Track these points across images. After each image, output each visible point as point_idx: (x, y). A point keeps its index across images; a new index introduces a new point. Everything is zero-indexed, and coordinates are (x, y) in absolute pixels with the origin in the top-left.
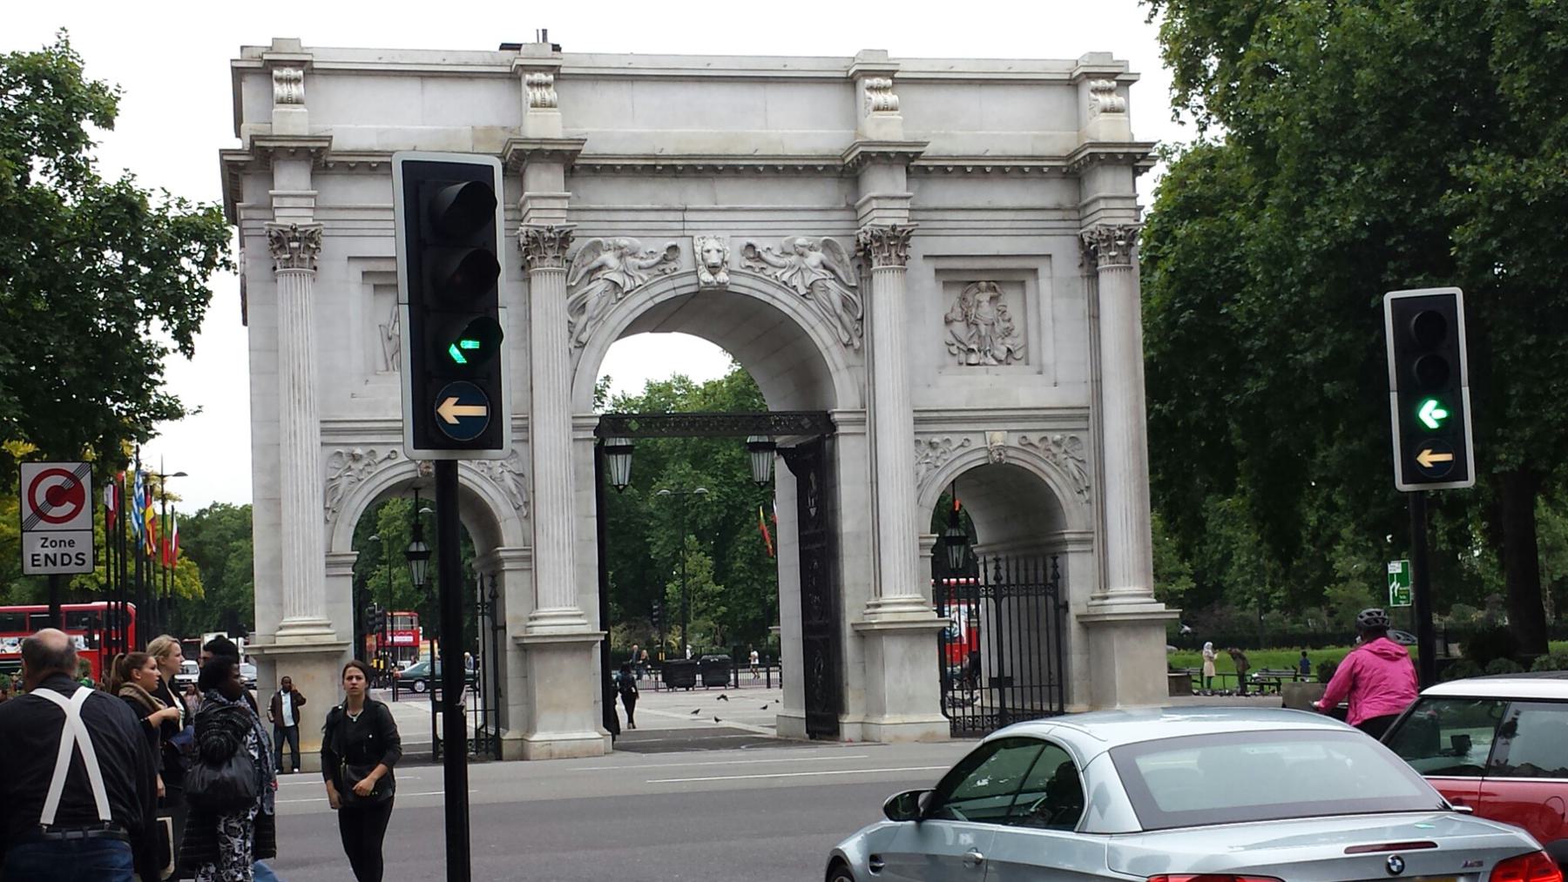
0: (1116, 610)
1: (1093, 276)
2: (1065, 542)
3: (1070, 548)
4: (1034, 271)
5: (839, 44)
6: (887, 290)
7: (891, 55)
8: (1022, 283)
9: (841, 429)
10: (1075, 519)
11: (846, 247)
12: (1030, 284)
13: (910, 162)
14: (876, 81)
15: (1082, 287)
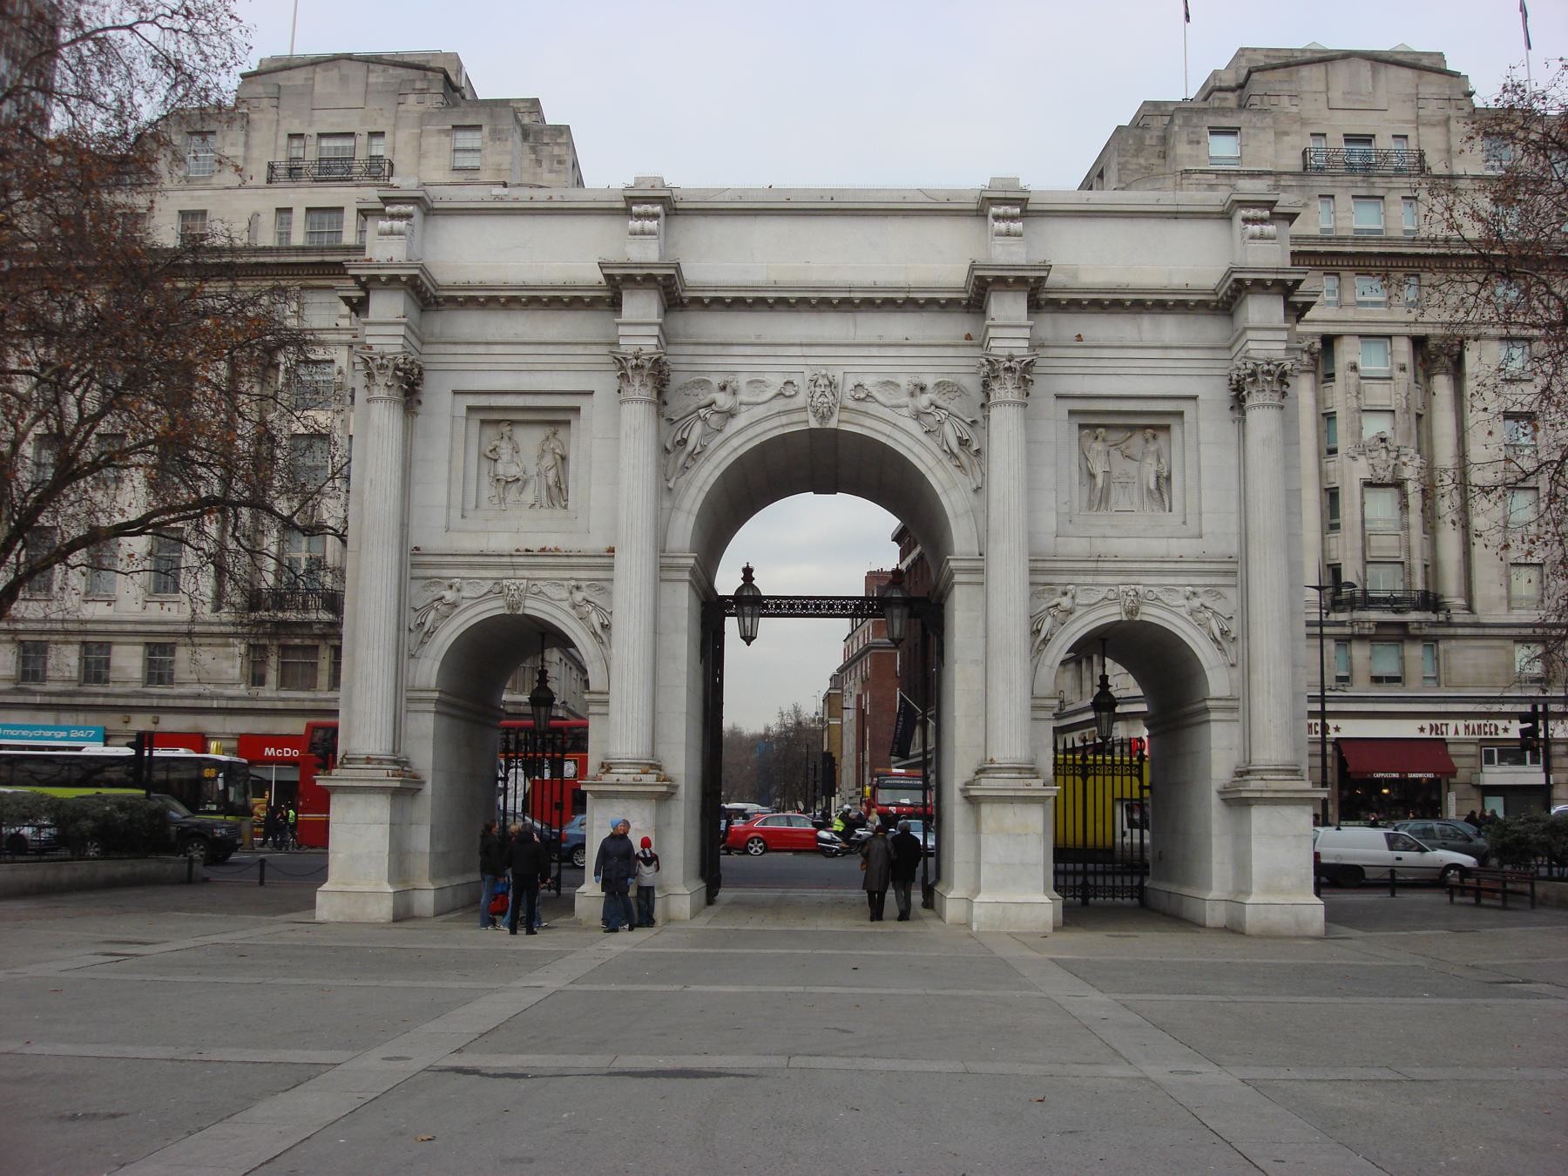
0: (1253, 785)
1: (1242, 421)
2: (1207, 710)
3: (1213, 716)
4: (1180, 414)
5: (969, 176)
6: (1005, 424)
7: (1022, 184)
8: (1167, 428)
9: (958, 578)
10: (1218, 681)
11: (972, 384)
12: (1176, 431)
13: (1039, 294)
14: (1001, 210)
15: (1232, 431)
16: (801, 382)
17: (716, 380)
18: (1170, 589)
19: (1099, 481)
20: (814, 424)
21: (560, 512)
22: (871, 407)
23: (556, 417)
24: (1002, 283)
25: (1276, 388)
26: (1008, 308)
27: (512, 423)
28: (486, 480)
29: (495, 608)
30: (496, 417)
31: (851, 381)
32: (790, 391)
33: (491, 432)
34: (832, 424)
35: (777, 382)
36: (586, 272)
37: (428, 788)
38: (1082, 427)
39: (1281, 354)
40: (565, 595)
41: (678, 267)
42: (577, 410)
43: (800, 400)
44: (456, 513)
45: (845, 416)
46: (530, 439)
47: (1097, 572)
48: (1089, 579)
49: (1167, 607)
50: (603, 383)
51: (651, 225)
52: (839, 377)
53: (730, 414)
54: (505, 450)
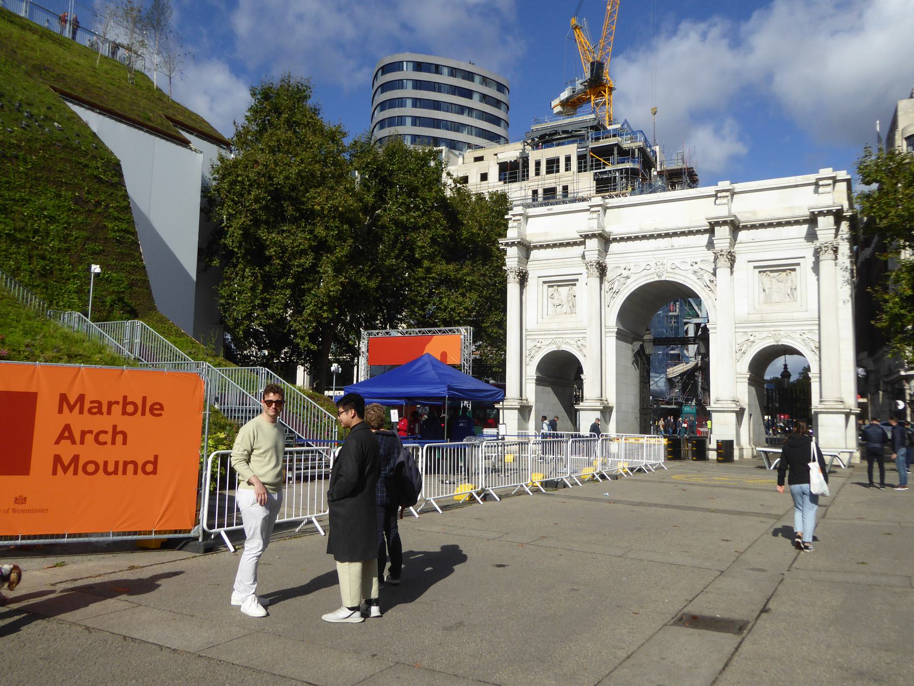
16: (653, 264)
17: (623, 266)
18: (794, 332)
19: (767, 291)
20: (657, 279)
21: (573, 315)
22: (677, 271)
23: (572, 283)
24: (718, 224)
25: (832, 252)
26: (723, 232)
27: (558, 286)
28: (550, 305)
29: (553, 348)
30: (553, 283)
31: (670, 263)
32: (648, 267)
33: (550, 289)
34: (663, 279)
35: (644, 266)
36: (573, 234)
37: (533, 409)
38: (760, 272)
39: (832, 239)
40: (573, 342)
41: (603, 230)
42: (577, 280)
43: (652, 271)
44: (540, 317)
45: (668, 275)
46: (564, 290)
47: (763, 327)
48: (760, 329)
49: (792, 338)
50: (583, 270)
51: (595, 215)
52: (665, 262)
53: (628, 278)
54: (556, 295)
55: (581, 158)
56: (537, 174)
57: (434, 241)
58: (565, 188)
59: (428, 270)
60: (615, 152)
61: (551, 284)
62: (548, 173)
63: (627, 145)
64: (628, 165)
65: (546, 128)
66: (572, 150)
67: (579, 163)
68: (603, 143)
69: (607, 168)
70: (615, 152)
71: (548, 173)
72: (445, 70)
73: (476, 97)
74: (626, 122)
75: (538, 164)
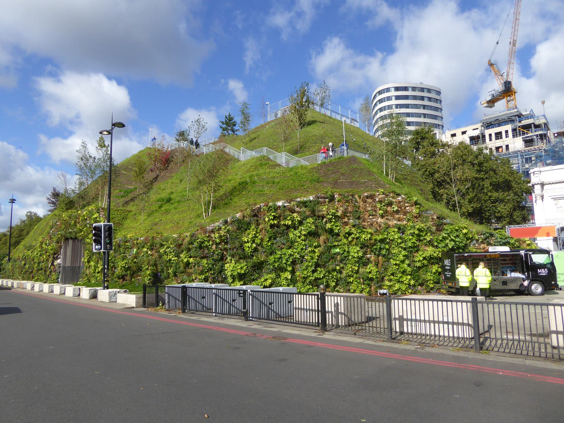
54: (558, 203)
55: (514, 130)
56: (490, 140)
57: (491, 184)
58: (507, 146)
59: (490, 197)
60: (533, 126)
61: (555, 199)
62: (496, 139)
63: (537, 123)
64: (541, 132)
65: (491, 118)
66: (509, 127)
67: (513, 133)
68: (524, 122)
69: (529, 135)
70: (533, 126)
71: (496, 139)
72: (410, 89)
73: (426, 99)
74: (532, 110)
75: (490, 135)
